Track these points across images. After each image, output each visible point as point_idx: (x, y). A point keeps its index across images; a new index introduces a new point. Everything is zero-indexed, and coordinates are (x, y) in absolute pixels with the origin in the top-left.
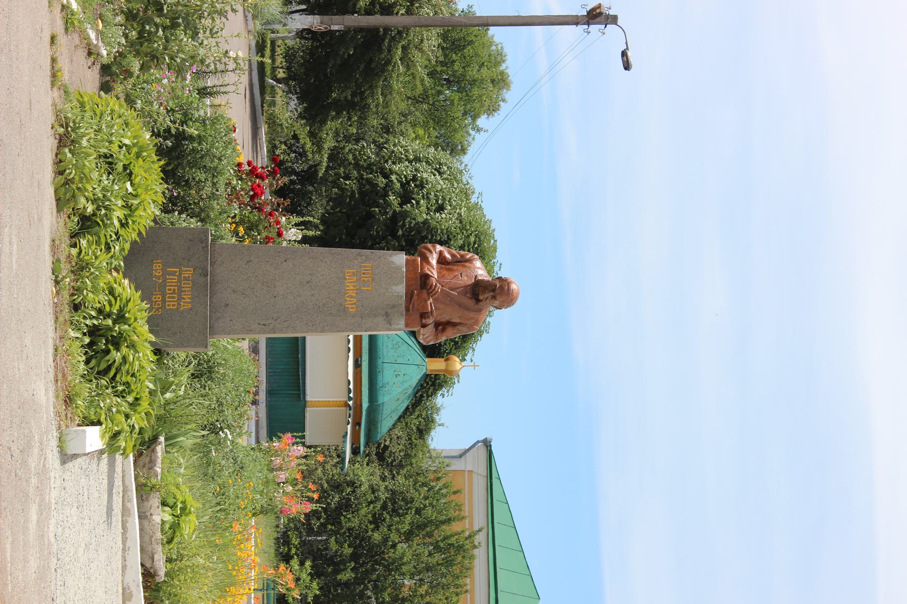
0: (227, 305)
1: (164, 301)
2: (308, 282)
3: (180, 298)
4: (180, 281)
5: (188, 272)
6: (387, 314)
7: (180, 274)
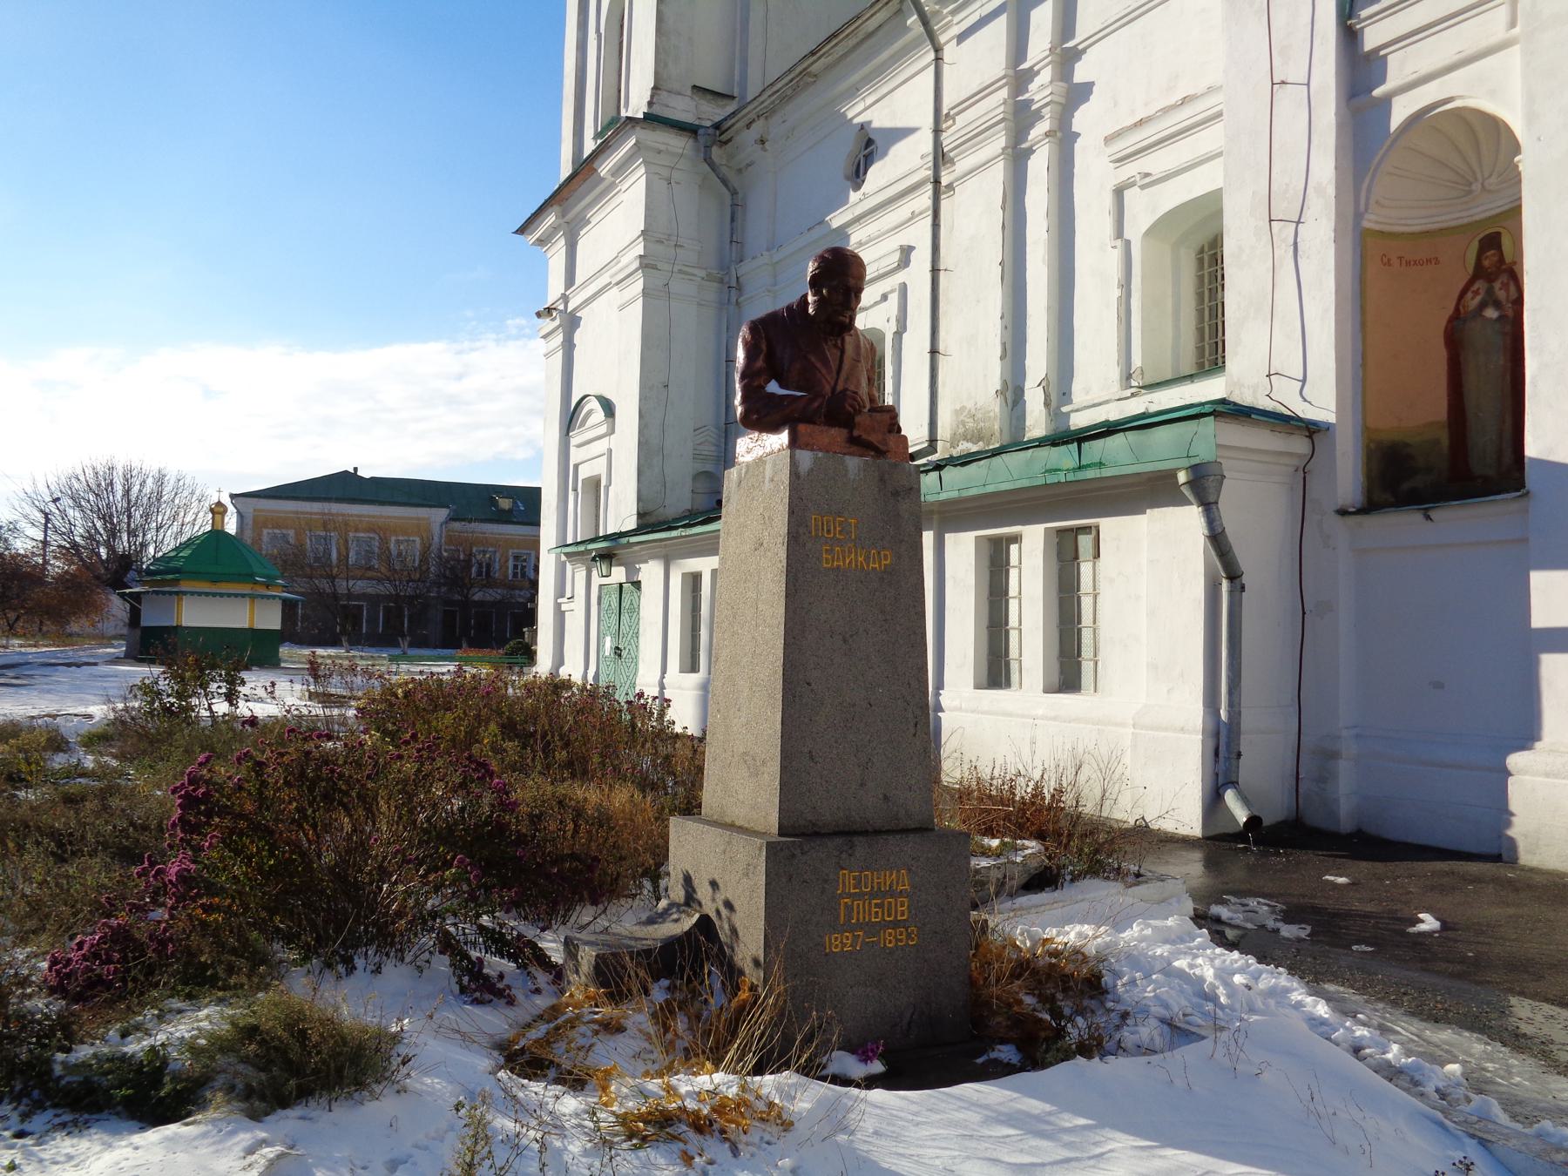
0: (886, 798)
1: (896, 924)
2: (845, 641)
3: (891, 893)
4: (861, 896)
5: (847, 878)
6: (896, 494)
7: (850, 895)
